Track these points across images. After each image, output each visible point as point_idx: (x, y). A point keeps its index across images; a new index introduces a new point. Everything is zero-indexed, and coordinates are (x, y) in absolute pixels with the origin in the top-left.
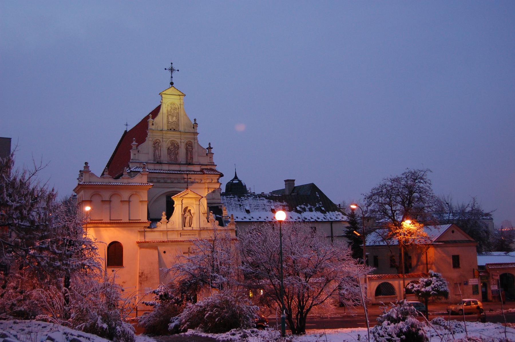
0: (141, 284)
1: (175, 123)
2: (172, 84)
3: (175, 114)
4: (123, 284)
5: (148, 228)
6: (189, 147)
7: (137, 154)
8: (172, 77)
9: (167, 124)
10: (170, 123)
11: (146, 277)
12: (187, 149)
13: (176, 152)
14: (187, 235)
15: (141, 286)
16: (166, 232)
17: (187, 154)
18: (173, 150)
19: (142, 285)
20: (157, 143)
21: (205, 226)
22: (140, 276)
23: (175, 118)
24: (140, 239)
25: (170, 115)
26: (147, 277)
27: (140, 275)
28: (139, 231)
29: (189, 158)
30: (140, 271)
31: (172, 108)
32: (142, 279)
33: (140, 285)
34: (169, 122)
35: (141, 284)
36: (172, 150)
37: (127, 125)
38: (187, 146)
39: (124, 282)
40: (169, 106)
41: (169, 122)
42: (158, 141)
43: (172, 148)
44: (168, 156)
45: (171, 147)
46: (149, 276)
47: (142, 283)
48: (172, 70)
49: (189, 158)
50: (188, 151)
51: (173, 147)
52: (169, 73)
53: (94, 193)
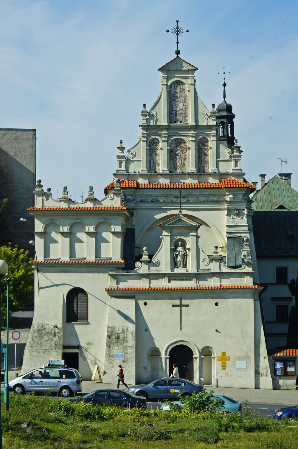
1: (182, 113)
3: (182, 99)
4: (87, 347)
5: (122, 269)
8: (178, 43)
9: (170, 114)
11: (116, 337)
15: (110, 350)
16: (149, 276)
19: (111, 349)
20: (154, 143)
21: (206, 268)
22: (109, 337)
24: (112, 284)
26: (118, 338)
27: (109, 335)
30: (109, 329)
32: (110, 341)
33: (108, 349)
34: (173, 111)
35: (109, 347)
38: (201, 145)
39: (89, 344)
41: (173, 111)
42: (156, 141)
46: (121, 336)
47: (112, 346)
48: (178, 31)
52: (172, 36)
53: (50, 222)
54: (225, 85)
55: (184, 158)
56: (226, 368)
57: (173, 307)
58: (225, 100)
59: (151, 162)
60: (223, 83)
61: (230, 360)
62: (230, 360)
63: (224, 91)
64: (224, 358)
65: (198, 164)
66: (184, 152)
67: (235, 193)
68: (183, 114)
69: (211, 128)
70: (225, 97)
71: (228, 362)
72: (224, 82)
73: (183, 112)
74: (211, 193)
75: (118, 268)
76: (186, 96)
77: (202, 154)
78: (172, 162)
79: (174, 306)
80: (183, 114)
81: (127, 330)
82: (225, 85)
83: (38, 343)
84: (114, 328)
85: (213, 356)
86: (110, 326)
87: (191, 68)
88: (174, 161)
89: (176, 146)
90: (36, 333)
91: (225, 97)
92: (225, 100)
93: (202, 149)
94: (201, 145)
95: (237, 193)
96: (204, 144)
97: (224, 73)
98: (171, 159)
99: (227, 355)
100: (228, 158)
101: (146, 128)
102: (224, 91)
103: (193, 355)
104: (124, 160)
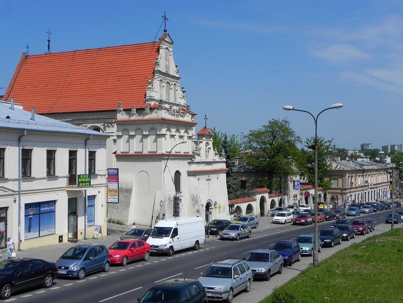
0: (194, 206)
2: (165, 31)
37: (28, 47)
47: (195, 206)
54: (49, 41)
58: (49, 50)
63: (49, 45)
64: (220, 207)
70: (49, 48)
71: (220, 209)
72: (49, 39)
76: (169, 58)
79: (207, 180)
82: (49, 41)
83: (170, 207)
84: (193, 195)
86: (192, 194)
87: (171, 42)
90: (168, 201)
91: (49, 48)
92: (49, 50)
100: (182, 97)
102: (49, 45)
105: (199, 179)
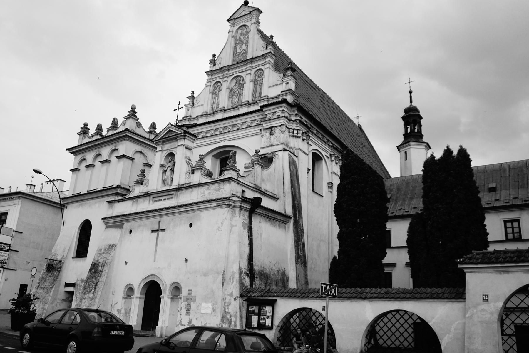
6: (259, 79)
7: (190, 109)
9: (234, 57)
10: (237, 54)
12: (255, 82)
13: (241, 91)
14: (161, 200)
17: (255, 89)
18: (237, 91)
23: (244, 45)
25: (238, 44)
28: (110, 202)
29: (257, 95)
31: (241, 34)
36: (235, 91)
38: (257, 77)
40: (239, 33)
41: (236, 53)
43: (236, 88)
44: (229, 100)
45: (235, 87)
49: (257, 95)
50: (257, 85)
51: (238, 86)
54: (411, 92)
55: (241, 93)
56: (190, 313)
57: (152, 233)
59: (213, 105)
60: (409, 90)
61: (195, 301)
62: (195, 301)
63: (411, 97)
65: (253, 96)
66: (241, 89)
67: (274, 111)
68: (245, 53)
69: (265, 58)
73: (245, 52)
74: (254, 119)
75: (117, 194)
77: (257, 86)
78: (231, 99)
79: (153, 231)
80: (245, 53)
81: (105, 262)
82: (411, 92)
85: (180, 296)
88: (232, 99)
89: (235, 85)
93: (258, 81)
94: (257, 77)
95: (275, 111)
96: (260, 75)
97: (410, 82)
98: (230, 98)
99: (193, 295)
100: (280, 82)
101: (210, 74)
102: (411, 97)
103: (161, 294)
104: (189, 108)
105: (131, 232)
